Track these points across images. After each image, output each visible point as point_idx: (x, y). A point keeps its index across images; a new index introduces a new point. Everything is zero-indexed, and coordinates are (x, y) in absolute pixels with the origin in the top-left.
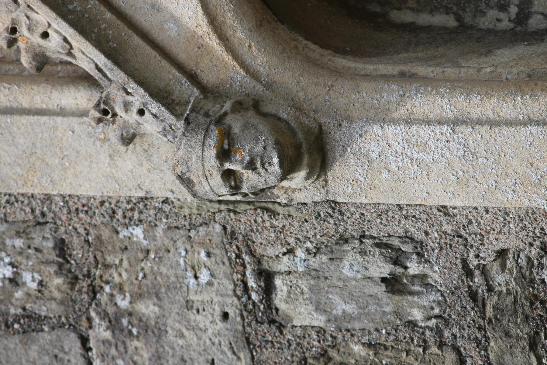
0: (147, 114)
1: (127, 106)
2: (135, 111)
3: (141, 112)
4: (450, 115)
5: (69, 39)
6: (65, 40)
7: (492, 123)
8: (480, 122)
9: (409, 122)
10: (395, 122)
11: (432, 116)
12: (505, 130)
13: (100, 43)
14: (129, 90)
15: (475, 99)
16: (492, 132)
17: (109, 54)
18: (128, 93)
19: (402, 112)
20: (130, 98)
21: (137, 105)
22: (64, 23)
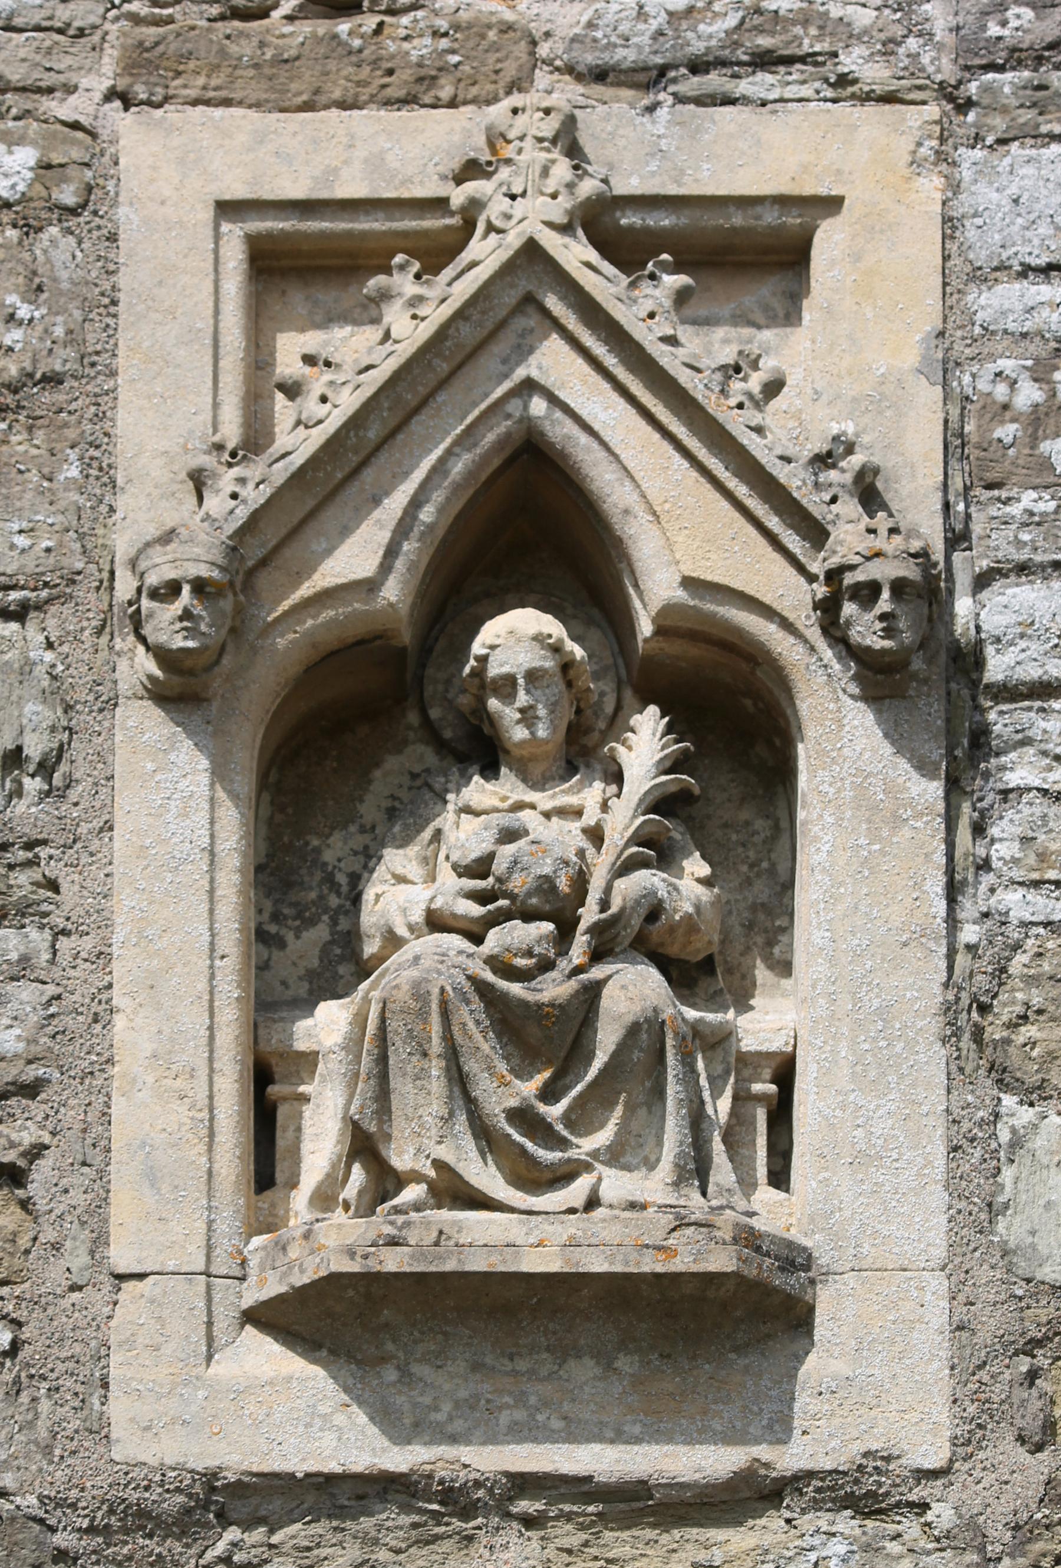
0: (233, 503)
1: (242, 481)
2: (237, 490)
3: (234, 496)
4: (218, 848)
5: (321, 426)
6: (320, 422)
7: (211, 892)
8: (212, 881)
9: (212, 800)
10: (212, 785)
11: (217, 827)
12: (205, 907)
13: (314, 462)
14: (261, 486)
15: (236, 878)
16: (203, 892)
17: (302, 470)
18: (258, 485)
19: (221, 794)
20: (251, 485)
21: (243, 493)
22: (340, 423)
